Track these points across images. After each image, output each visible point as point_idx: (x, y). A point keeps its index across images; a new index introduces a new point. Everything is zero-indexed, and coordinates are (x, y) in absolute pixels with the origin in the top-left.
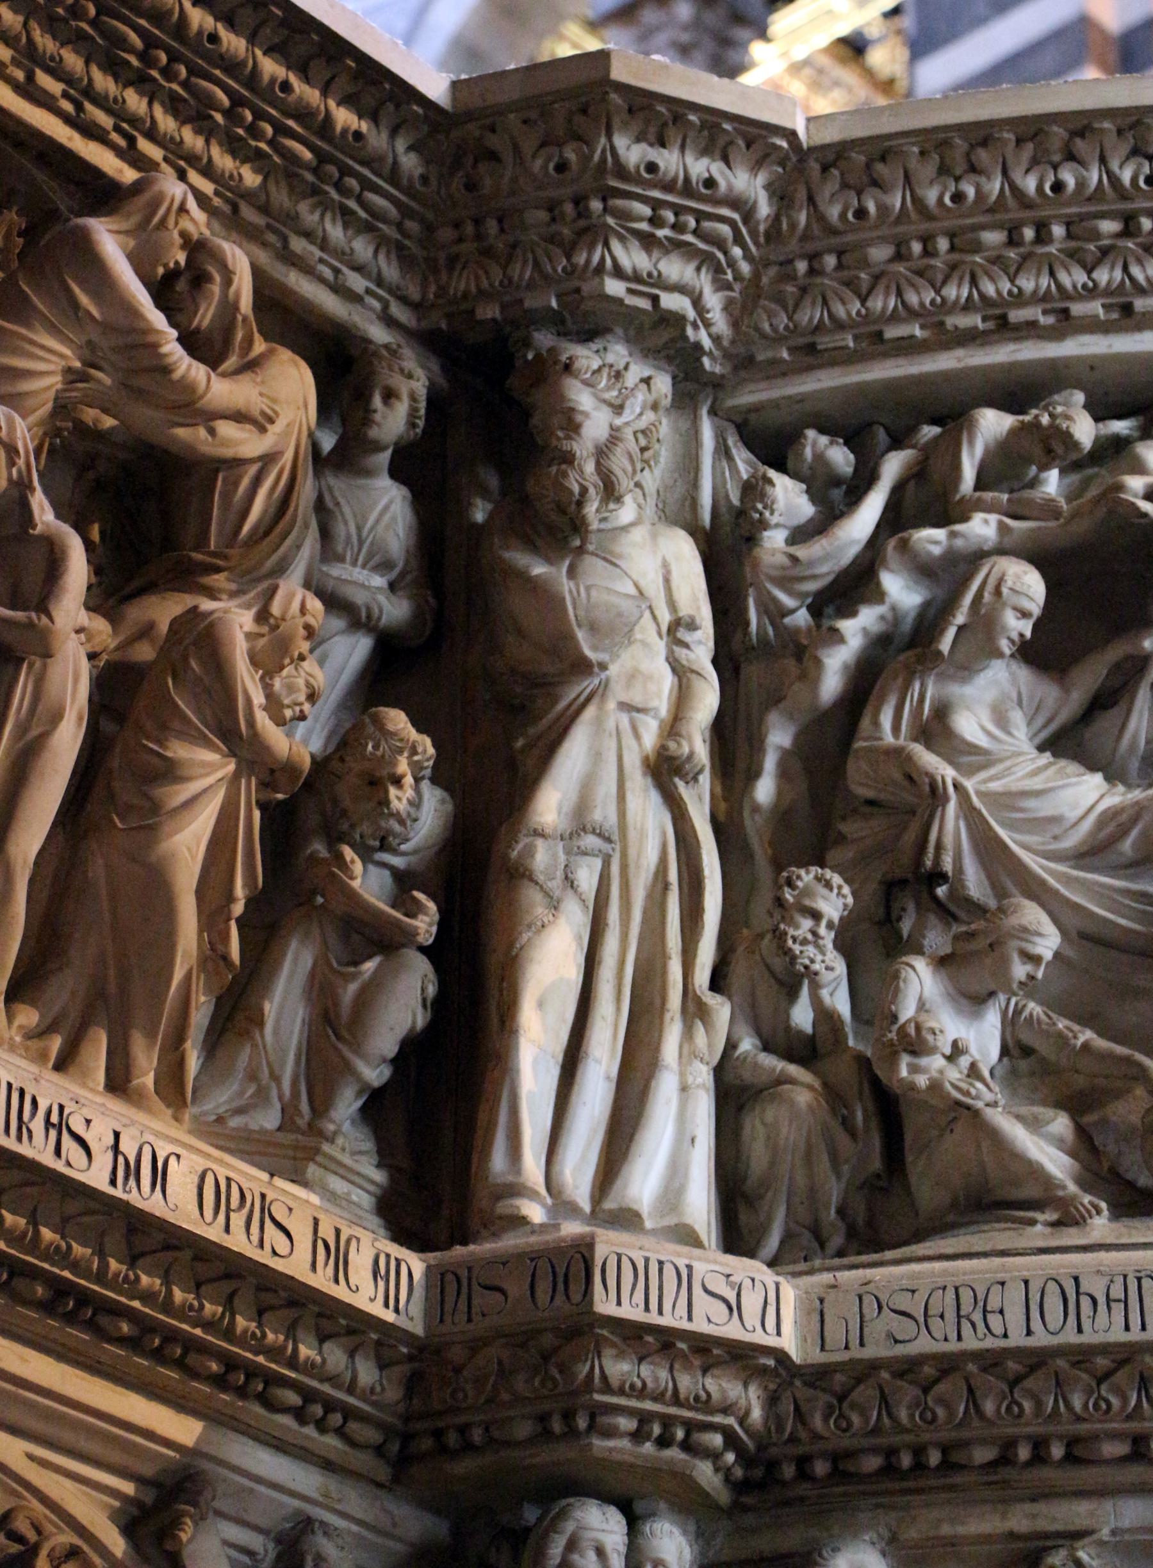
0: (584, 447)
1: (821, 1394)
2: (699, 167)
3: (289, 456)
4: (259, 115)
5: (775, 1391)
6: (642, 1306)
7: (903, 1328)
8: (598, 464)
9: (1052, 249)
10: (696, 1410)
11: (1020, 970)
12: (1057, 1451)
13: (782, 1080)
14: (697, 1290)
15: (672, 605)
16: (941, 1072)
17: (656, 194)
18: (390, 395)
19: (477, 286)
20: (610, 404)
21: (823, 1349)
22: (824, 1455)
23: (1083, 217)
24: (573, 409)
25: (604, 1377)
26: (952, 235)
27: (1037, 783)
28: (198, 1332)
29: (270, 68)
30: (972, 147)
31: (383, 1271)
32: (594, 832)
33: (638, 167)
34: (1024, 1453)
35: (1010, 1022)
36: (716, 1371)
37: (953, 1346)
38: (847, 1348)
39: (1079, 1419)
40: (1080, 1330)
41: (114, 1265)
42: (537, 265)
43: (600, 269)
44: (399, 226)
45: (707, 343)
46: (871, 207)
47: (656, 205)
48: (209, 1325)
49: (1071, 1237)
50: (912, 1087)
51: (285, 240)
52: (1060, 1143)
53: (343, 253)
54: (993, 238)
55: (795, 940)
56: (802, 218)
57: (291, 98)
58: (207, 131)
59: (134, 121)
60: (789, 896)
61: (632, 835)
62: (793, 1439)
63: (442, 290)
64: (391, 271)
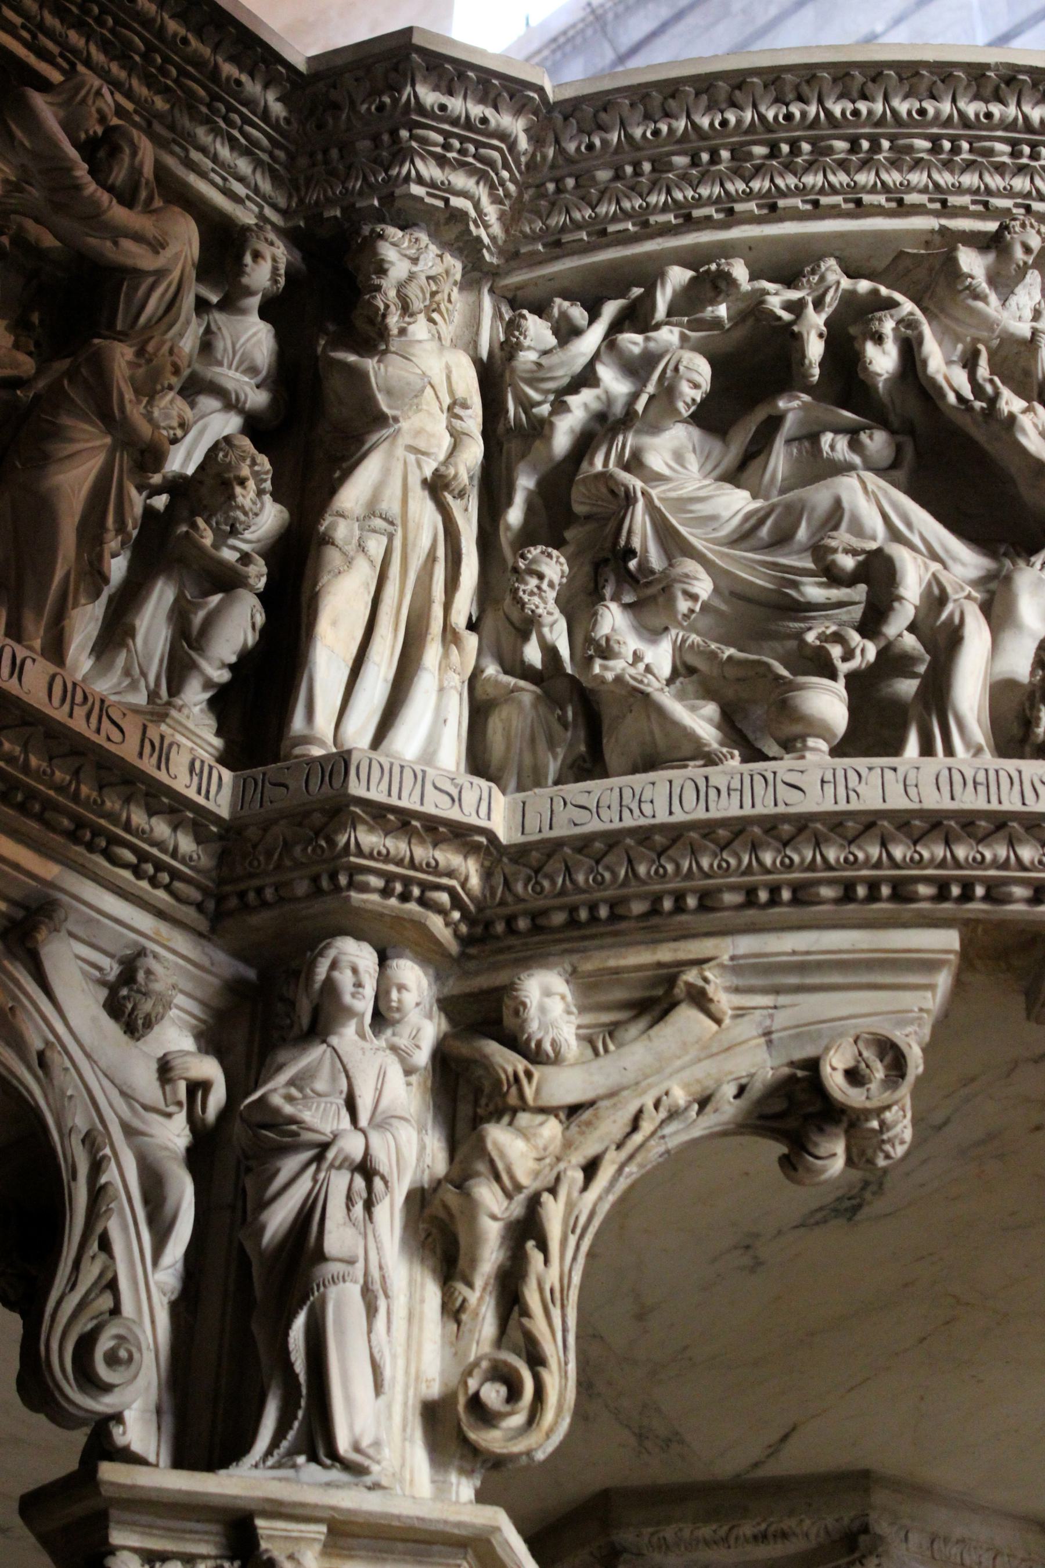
0: (389, 286)
1: (521, 868)
2: (477, 110)
3: (176, 275)
4: (166, 60)
5: (489, 868)
6: (386, 792)
8: (398, 291)
9: (721, 167)
10: (428, 873)
11: (683, 605)
12: (691, 902)
13: (516, 689)
14: (429, 787)
15: (451, 392)
16: (623, 670)
17: (446, 127)
18: (257, 256)
19: (324, 195)
20: (410, 258)
21: (523, 833)
22: (525, 913)
23: (743, 144)
24: (383, 260)
25: (357, 844)
26: (653, 162)
27: (702, 493)
28: (51, 793)
29: (173, 26)
30: (665, 99)
31: (197, 770)
32: (381, 517)
33: (432, 107)
34: (668, 904)
35: (679, 649)
36: (441, 846)
37: (617, 825)
38: (540, 831)
39: (707, 876)
40: (707, 810)
42: (365, 179)
43: (407, 179)
44: (271, 155)
45: (486, 240)
46: (597, 142)
47: (447, 135)
48: (61, 789)
50: (602, 680)
51: (187, 151)
52: (710, 721)
53: (229, 166)
54: (681, 161)
55: (524, 592)
56: (551, 152)
57: (189, 49)
58: (130, 68)
59: (75, 51)
60: (522, 564)
61: (411, 525)
62: (502, 903)
63: (301, 201)
64: (266, 186)
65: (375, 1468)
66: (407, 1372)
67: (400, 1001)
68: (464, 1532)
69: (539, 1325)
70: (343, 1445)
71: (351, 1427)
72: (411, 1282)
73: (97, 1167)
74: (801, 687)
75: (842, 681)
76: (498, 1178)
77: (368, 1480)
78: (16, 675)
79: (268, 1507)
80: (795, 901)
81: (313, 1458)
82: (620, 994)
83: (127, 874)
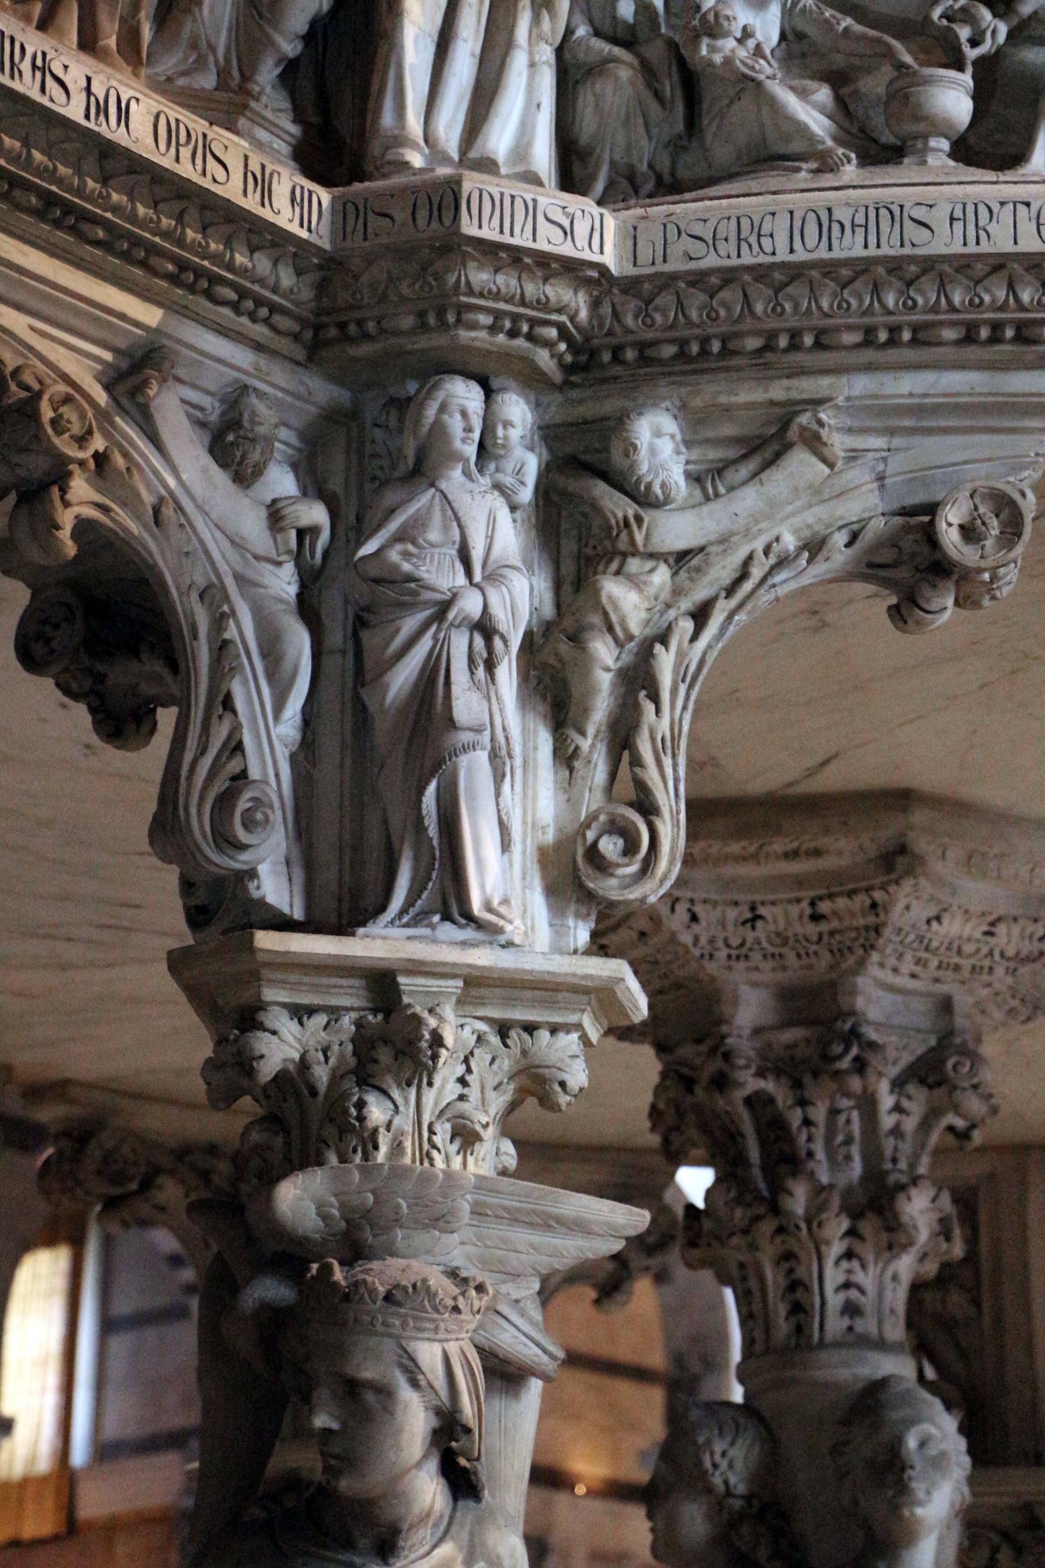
5: (597, 297)
6: (498, 229)
7: (696, 248)
10: (538, 310)
12: (808, 340)
14: (540, 219)
16: (733, 51)
21: (635, 265)
22: (634, 344)
25: (468, 283)
28: (157, 239)
31: (298, 199)
34: (783, 342)
36: (552, 281)
37: (734, 262)
38: (653, 263)
39: (826, 315)
40: (830, 249)
41: (90, 183)
48: (165, 235)
49: (828, 180)
50: (710, 64)
62: (610, 333)
65: (509, 928)
66: (524, 822)
67: (506, 438)
68: (590, 983)
69: (651, 775)
70: (476, 906)
71: (482, 887)
72: (524, 730)
73: (219, 621)
74: (927, 81)
75: (969, 70)
76: (610, 629)
77: (502, 939)
78: (123, 123)
79: (410, 966)
80: (915, 342)
81: (447, 917)
82: (728, 430)
83: (226, 311)
